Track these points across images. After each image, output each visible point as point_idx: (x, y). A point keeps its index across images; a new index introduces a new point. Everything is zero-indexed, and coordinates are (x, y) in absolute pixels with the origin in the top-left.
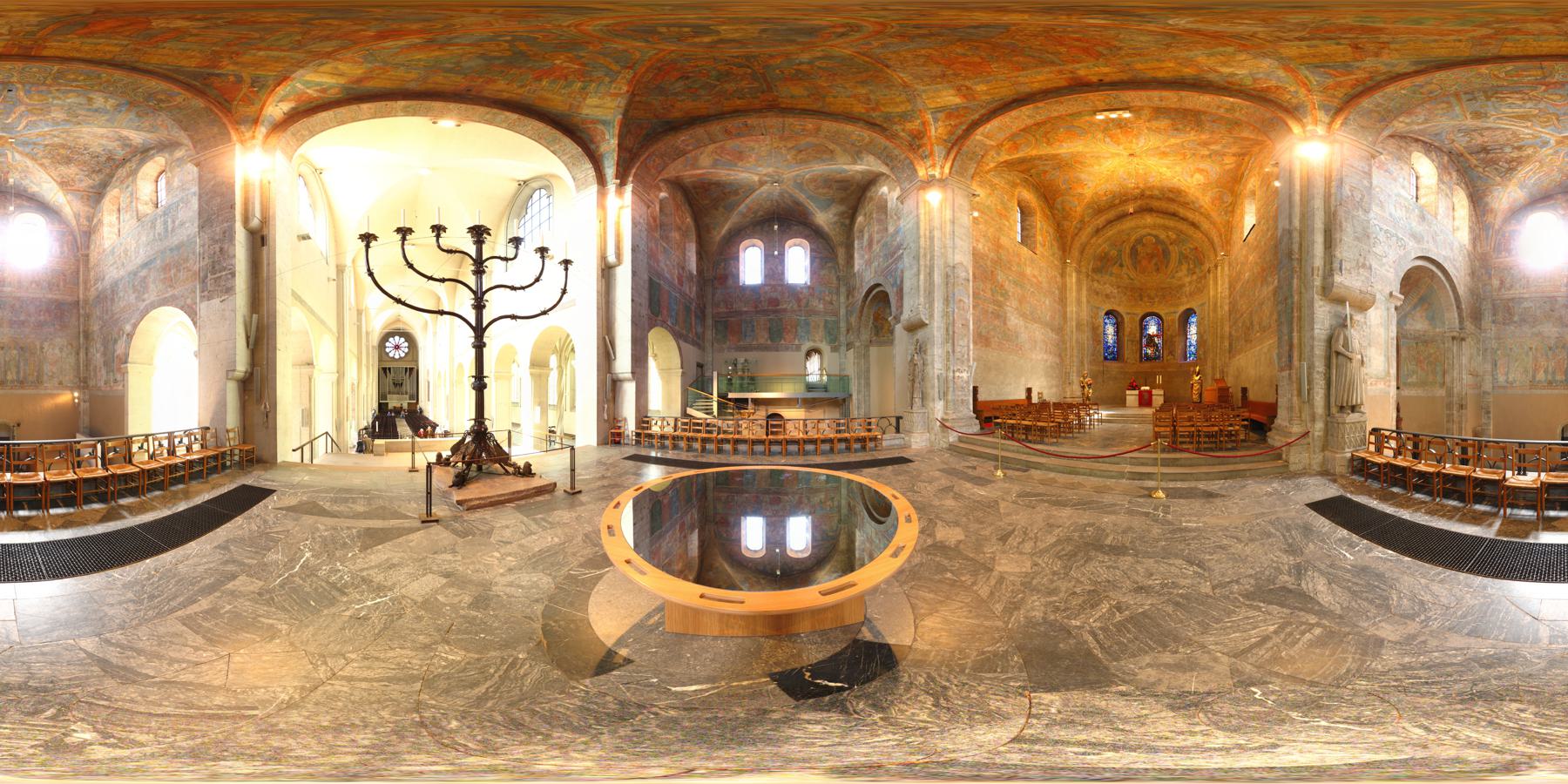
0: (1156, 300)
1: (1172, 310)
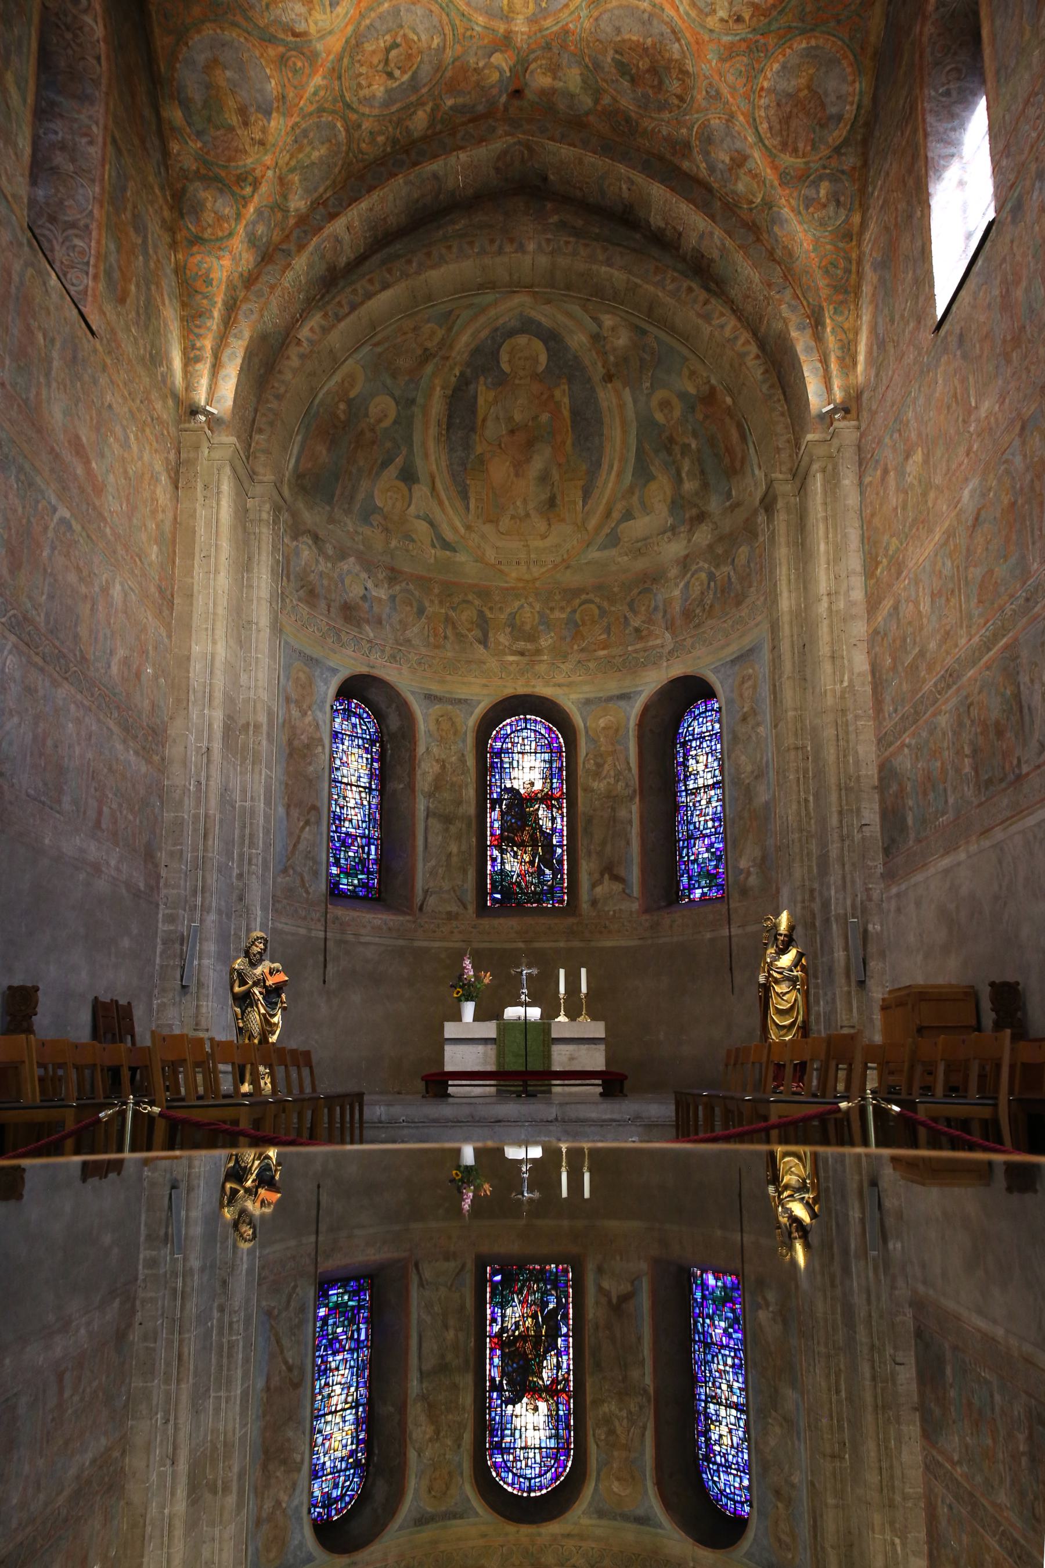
0: (545, 641)
1: (612, 686)
